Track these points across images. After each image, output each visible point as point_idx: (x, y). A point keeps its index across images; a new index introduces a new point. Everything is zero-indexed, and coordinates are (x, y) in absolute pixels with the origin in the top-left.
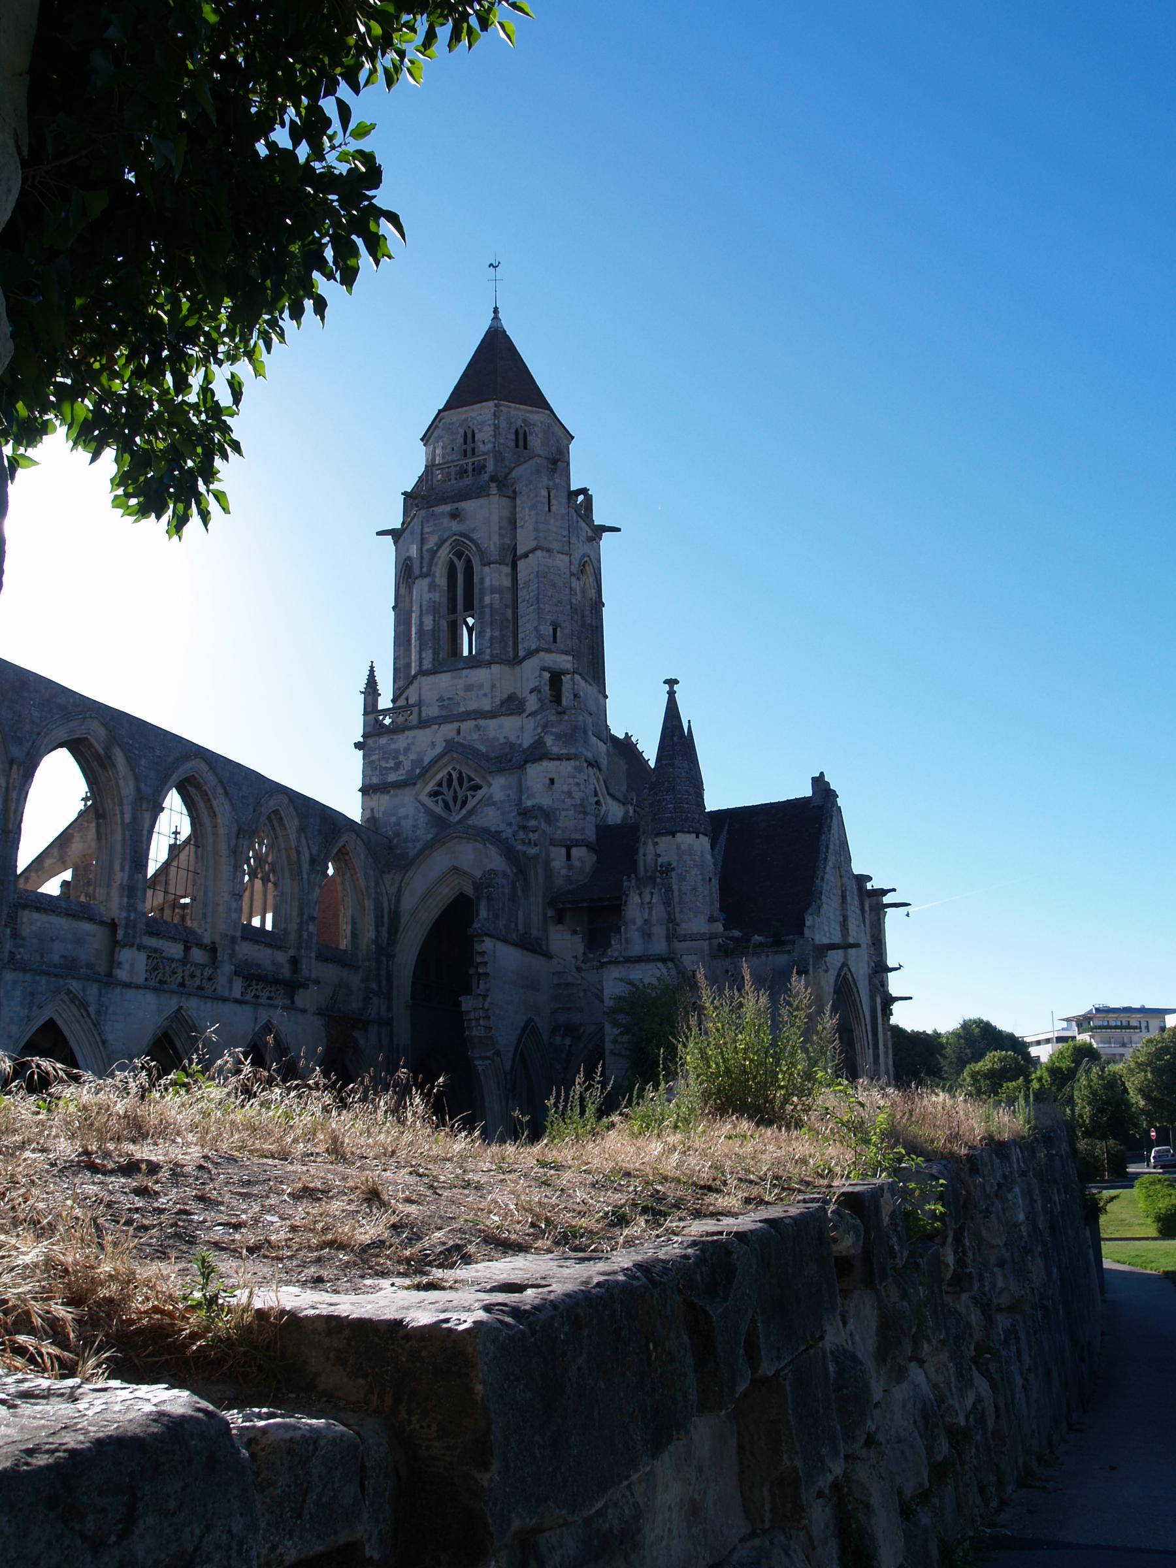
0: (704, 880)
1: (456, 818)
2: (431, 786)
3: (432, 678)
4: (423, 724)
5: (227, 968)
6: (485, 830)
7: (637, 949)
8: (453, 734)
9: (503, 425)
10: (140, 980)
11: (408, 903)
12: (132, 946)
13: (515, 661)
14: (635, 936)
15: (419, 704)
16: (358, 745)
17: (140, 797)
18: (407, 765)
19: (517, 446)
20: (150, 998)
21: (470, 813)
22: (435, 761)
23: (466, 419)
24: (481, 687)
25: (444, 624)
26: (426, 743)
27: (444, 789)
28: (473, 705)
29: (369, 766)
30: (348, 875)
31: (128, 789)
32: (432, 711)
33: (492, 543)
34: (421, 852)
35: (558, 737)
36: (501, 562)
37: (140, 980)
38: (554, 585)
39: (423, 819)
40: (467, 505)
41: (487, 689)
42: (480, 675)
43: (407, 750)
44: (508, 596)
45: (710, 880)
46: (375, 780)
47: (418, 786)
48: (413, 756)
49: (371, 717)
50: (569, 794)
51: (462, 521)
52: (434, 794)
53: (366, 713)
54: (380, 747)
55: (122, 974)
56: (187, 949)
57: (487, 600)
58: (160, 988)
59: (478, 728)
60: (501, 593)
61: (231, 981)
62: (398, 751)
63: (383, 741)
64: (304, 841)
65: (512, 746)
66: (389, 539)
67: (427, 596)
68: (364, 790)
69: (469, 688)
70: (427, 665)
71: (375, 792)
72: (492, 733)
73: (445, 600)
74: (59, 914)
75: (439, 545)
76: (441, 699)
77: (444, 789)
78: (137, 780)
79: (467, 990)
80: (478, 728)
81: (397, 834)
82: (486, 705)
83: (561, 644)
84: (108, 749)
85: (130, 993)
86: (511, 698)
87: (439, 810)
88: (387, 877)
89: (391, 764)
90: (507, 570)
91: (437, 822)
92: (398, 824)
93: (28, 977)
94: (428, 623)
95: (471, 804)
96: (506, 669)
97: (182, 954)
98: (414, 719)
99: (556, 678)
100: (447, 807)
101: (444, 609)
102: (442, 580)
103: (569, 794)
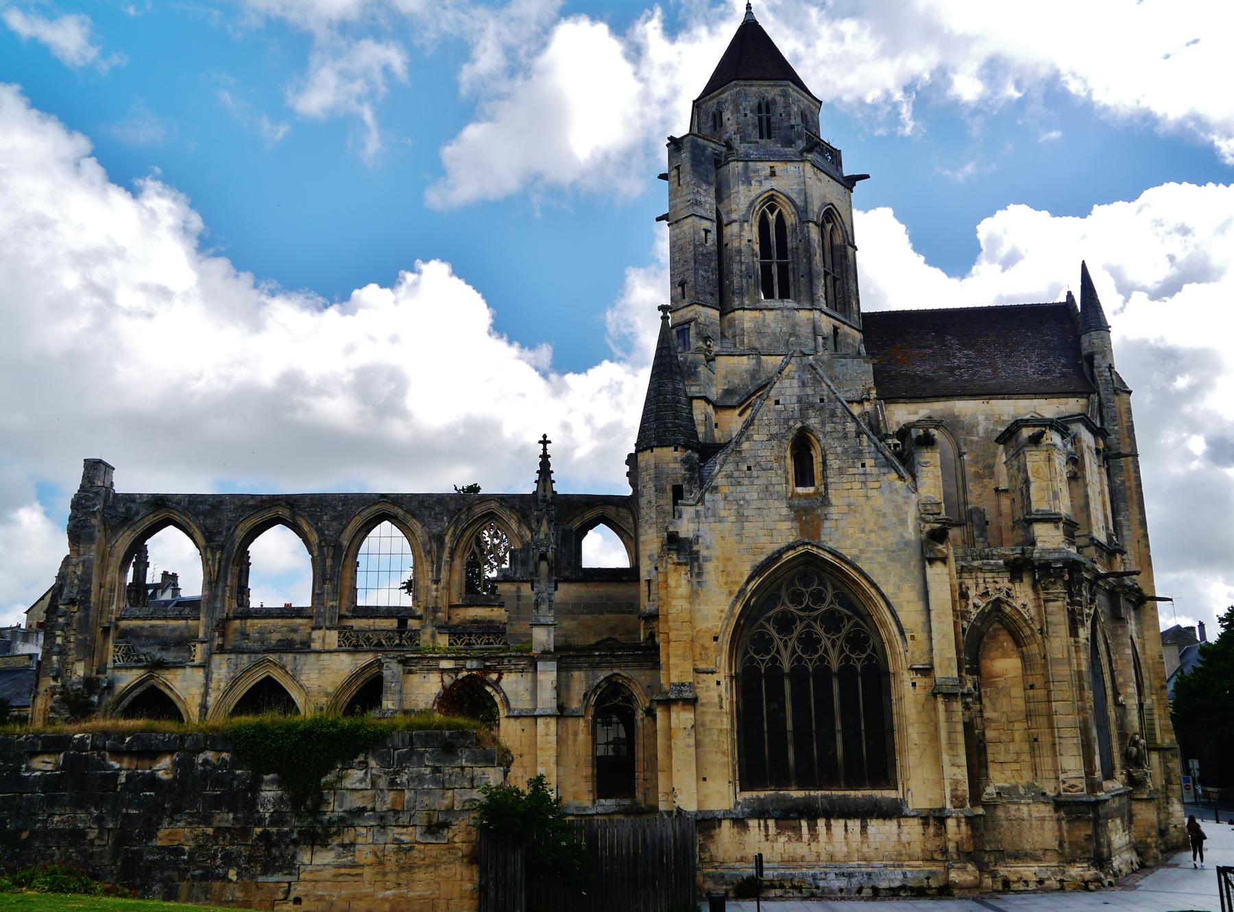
0: (659, 490)
5: (429, 630)
10: (335, 646)
12: (320, 628)
20: (343, 656)
31: (314, 538)
37: (335, 646)
55: (316, 646)
56: (403, 623)
58: (355, 649)
61: (433, 636)
64: (525, 528)
74: (273, 618)
78: (320, 531)
84: (293, 518)
85: (325, 656)
93: (233, 656)
97: (396, 624)
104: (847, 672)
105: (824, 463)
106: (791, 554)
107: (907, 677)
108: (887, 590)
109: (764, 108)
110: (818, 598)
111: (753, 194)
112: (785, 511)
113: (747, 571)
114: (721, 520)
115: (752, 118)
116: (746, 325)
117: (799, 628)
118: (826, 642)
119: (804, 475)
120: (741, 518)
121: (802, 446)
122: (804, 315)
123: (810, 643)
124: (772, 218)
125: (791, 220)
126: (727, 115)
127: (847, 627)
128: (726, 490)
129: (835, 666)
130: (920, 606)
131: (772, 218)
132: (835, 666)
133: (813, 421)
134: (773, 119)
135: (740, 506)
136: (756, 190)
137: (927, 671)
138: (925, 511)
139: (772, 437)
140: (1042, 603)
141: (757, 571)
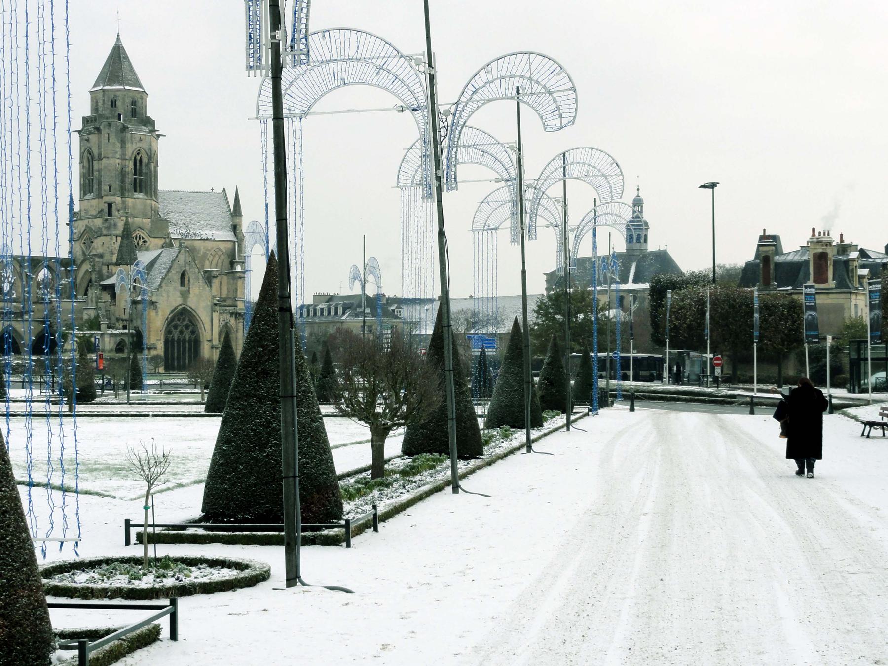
9: (106, 99)
13: (102, 197)
16: (67, 225)
33: (95, 152)
82: (94, 213)
83: (112, 193)
86: (102, 210)
91: (84, 253)
99: (110, 205)
102: (86, 164)
104: (190, 340)
107: (206, 343)
108: (203, 319)
110: (184, 320)
112: (179, 294)
113: (168, 312)
115: (130, 107)
116: (130, 205)
117: (179, 328)
118: (185, 332)
119: (182, 283)
120: (168, 296)
121: (183, 275)
122: (148, 202)
123: (181, 332)
124: (138, 158)
125: (145, 160)
127: (191, 328)
129: (187, 338)
131: (138, 158)
132: (187, 338)
133: (188, 268)
134: (137, 109)
136: (134, 146)
137: (210, 341)
138: (213, 297)
140: (237, 323)
141: (172, 312)
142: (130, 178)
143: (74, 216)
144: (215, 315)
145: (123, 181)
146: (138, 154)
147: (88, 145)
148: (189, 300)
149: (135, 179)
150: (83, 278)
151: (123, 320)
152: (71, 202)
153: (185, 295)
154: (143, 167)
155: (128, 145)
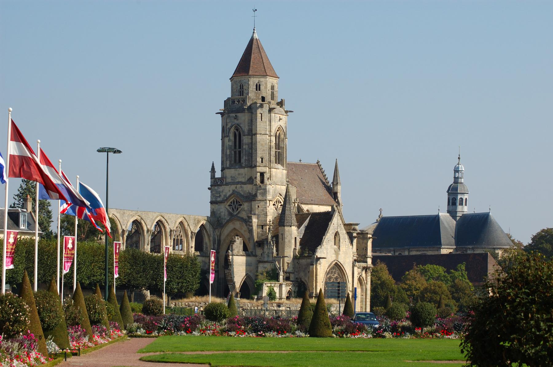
1: (235, 214)
2: (229, 203)
3: (229, 170)
4: (227, 184)
6: (242, 218)
7: (266, 259)
8: (234, 188)
11: (223, 238)
14: (266, 256)
15: (226, 178)
16: (209, 189)
17: (148, 231)
18: (222, 196)
19: (257, 90)
21: (239, 213)
22: (230, 196)
23: (240, 81)
24: (242, 174)
25: (233, 153)
26: (227, 190)
27: (232, 204)
28: (240, 180)
29: (212, 195)
30: (204, 231)
32: (229, 180)
34: (226, 223)
35: (260, 194)
36: (248, 135)
38: (262, 145)
39: (227, 213)
40: (239, 115)
41: (244, 175)
42: (242, 171)
43: (222, 191)
44: (250, 145)
45: (296, 238)
46: (214, 200)
47: (225, 203)
48: (224, 194)
49: (213, 180)
50: (263, 210)
51: (237, 120)
52: (230, 205)
53: (211, 178)
54: (215, 190)
57: (244, 147)
59: (241, 187)
60: (248, 145)
62: (220, 191)
63: (216, 188)
65: (250, 193)
66: (220, 115)
67: (228, 143)
68: (212, 203)
69: (239, 174)
70: (228, 166)
71: (214, 203)
72: (245, 189)
73: (233, 145)
75: (231, 127)
76: (231, 177)
77: (232, 204)
79: (227, 269)
80: (241, 187)
81: (220, 217)
82: (243, 180)
83: (264, 164)
87: (231, 211)
88: (216, 230)
89: (218, 195)
90: (250, 137)
91: (230, 214)
92: (220, 214)
94: (228, 153)
95: (239, 210)
96: (249, 169)
98: (224, 183)
100: (233, 209)
101: (233, 148)
103: (263, 210)
105: (339, 240)
106: (334, 262)
109: (273, 88)
111: (276, 126)
113: (327, 265)
114: (324, 253)
116: (274, 174)
125: (282, 136)
126: (262, 87)
128: (325, 246)
130: (351, 276)
133: (339, 230)
134: (275, 93)
135: (327, 249)
139: (333, 233)
141: (329, 266)
142: (273, 150)
143: (216, 183)
144: (356, 268)
145: (270, 154)
146: (278, 130)
147: (236, 121)
148: (340, 256)
149: (276, 152)
150: (228, 235)
151: (286, 273)
152: (213, 170)
153: (337, 253)
154: (280, 143)
155: (273, 123)
